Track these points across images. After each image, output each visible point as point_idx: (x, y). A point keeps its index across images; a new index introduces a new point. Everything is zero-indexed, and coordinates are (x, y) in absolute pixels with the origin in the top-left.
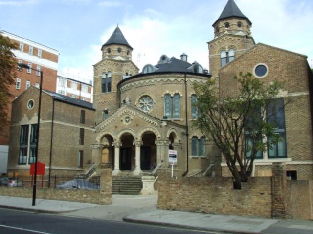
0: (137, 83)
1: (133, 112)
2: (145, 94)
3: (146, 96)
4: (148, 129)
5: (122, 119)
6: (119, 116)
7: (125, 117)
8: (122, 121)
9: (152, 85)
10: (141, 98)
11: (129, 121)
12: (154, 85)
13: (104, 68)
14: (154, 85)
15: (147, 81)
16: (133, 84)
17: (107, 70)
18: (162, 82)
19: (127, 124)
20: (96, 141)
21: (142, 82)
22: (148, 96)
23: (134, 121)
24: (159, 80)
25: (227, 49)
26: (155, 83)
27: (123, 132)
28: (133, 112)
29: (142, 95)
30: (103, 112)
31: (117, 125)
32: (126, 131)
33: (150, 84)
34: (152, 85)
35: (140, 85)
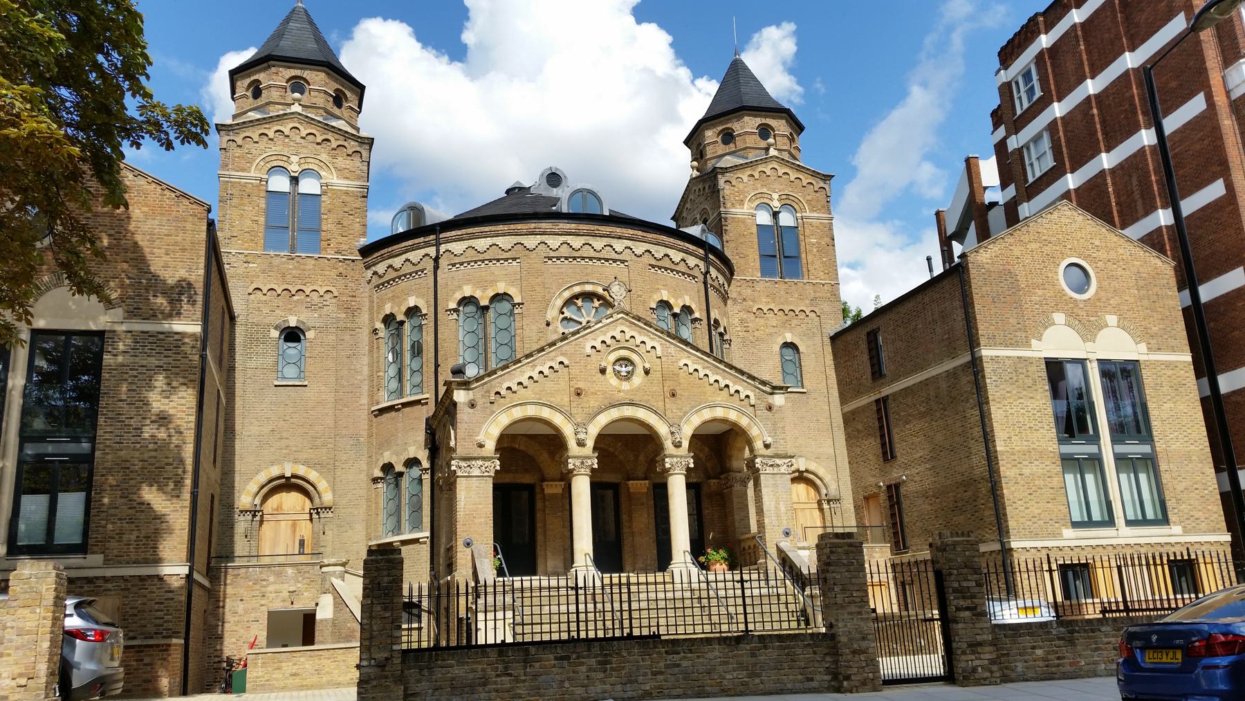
0: (554, 242)
1: (649, 344)
2: (589, 288)
3: (588, 296)
4: (719, 413)
5: (604, 364)
6: (589, 350)
7: (613, 357)
8: (603, 371)
9: (615, 261)
10: (569, 302)
11: (629, 375)
12: (623, 262)
13: (276, 149)
14: (623, 262)
15: (598, 243)
16: (531, 242)
17: (294, 159)
18: (647, 259)
19: (625, 386)
20: (481, 446)
21: (577, 242)
22: (599, 297)
23: (656, 375)
24: (640, 248)
25: (776, 204)
26: (627, 255)
27: (615, 414)
28: (649, 344)
29: (577, 289)
30: (275, 334)
31: (580, 385)
32: (628, 412)
33: (603, 254)
34: (615, 261)
35: (565, 251)
